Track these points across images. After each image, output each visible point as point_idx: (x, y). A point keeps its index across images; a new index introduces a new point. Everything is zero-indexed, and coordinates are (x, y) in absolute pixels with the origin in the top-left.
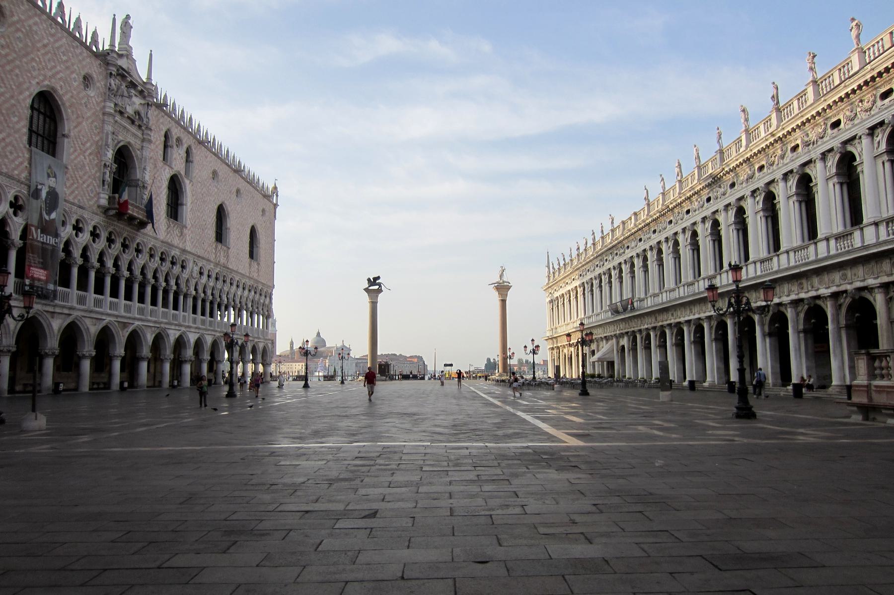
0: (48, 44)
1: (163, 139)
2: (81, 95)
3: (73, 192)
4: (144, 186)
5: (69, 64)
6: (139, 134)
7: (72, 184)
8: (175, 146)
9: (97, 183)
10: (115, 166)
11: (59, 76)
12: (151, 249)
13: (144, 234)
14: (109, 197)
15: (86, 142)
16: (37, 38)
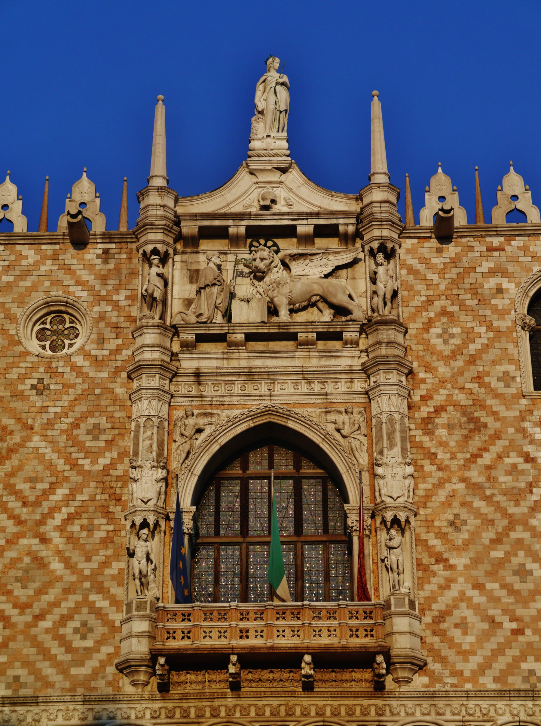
2: (13, 375)
15: (46, 494)
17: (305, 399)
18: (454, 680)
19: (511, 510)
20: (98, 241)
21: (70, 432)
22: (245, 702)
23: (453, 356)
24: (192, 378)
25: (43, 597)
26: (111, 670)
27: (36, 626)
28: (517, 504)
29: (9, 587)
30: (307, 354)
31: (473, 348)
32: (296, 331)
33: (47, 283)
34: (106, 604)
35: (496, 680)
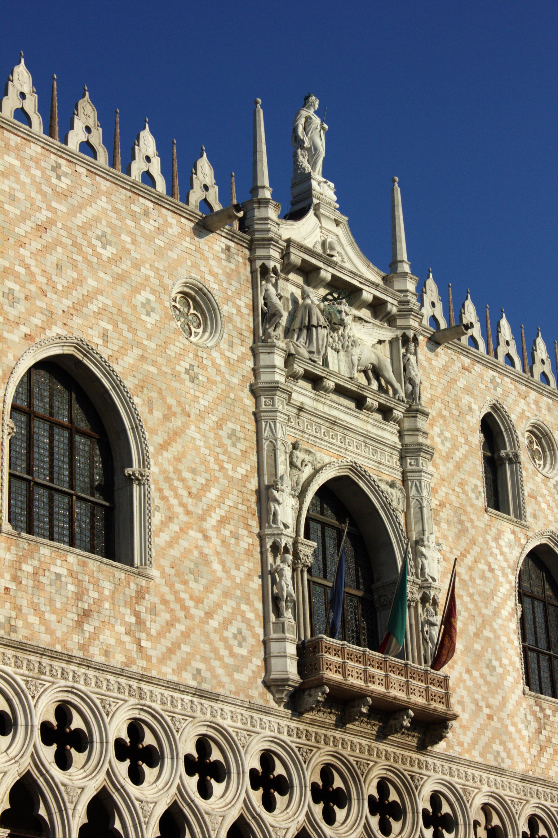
0: (52, 222)
1: (477, 438)
2: (172, 351)
3: (171, 651)
4: (425, 599)
5: (126, 265)
6: (389, 434)
7: (170, 624)
8: (524, 456)
9: (253, 609)
10: (308, 549)
11: (93, 307)
12: (486, 808)
13: (450, 759)
14: (302, 649)
16: (13, 210)
17: (369, 463)
18: (458, 749)
19: (484, 611)
20: (223, 234)
21: (216, 431)
22: (347, 737)
23: (448, 457)
24: (295, 411)
25: (210, 595)
26: (260, 681)
27: (208, 623)
28: (486, 607)
29: (186, 577)
30: (366, 418)
31: (458, 455)
32: (368, 395)
33: (189, 263)
34: (250, 615)
35: (482, 755)
